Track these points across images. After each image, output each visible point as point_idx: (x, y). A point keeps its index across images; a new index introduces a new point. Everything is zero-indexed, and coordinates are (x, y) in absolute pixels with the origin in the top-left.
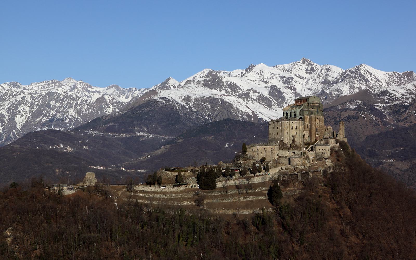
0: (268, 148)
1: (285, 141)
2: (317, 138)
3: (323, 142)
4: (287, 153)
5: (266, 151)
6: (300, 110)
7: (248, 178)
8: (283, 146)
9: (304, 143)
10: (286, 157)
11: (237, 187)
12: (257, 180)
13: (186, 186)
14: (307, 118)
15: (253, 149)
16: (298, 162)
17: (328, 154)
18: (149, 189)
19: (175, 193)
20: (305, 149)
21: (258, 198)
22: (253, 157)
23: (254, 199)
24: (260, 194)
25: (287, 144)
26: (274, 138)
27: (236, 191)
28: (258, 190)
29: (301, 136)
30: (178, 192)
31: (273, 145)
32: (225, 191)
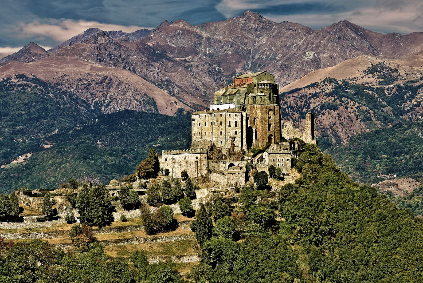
0: (191, 157)
1: (218, 145)
5: (187, 162)
15: (166, 160)
20: (250, 158)
25: (220, 151)
26: (200, 141)
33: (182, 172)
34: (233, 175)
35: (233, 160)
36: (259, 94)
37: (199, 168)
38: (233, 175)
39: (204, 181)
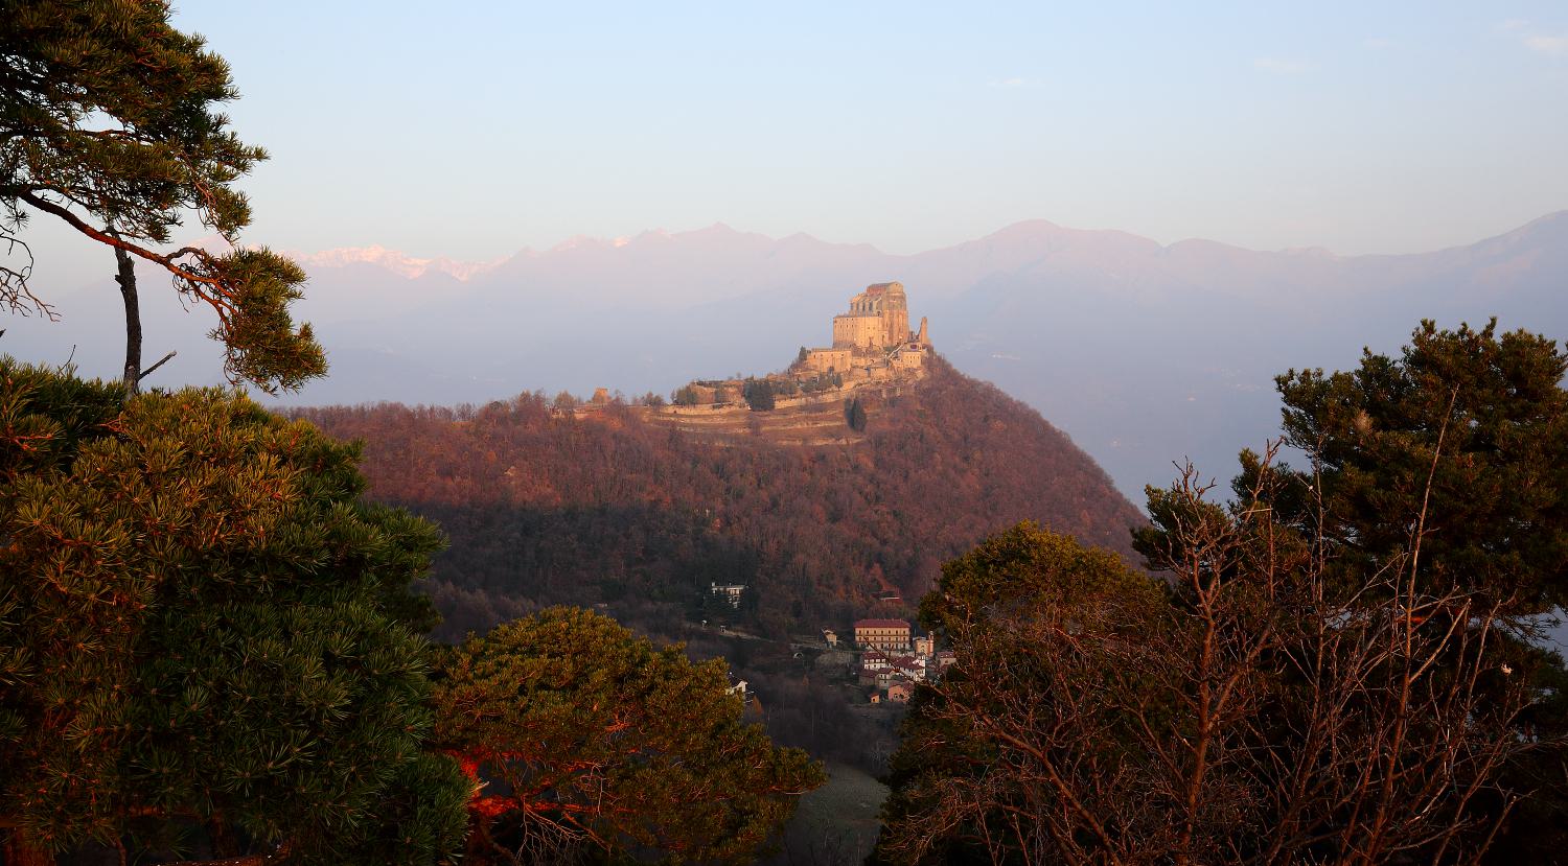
0: (838, 354)
3: (908, 346)
4: (862, 362)
7: (815, 396)
8: (857, 352)
10: (862, 367)
11: (802, 408)
12: (829, 398)
18: (681, 411)
22: (816, 366)
24: (833, 418)
27: (804, 414)
28: (829, 413)
30: (722, 416)
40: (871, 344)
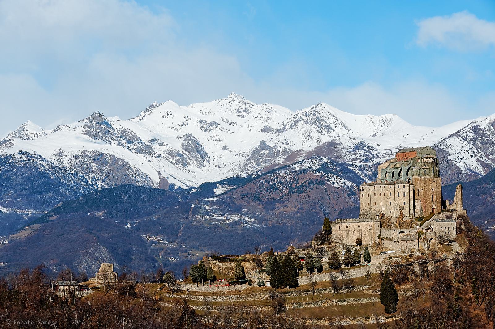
0: (365, 226)
2: (433, 211)
5: (361, 230)
6: (408, 168)
7: (342, 273)
9: (415, 217)
13: (250, 284)
14: (418, 180)
16: (413, 246)
17: (454, 234)
18: (194, 288)
19: (235, 292)
20: (418, 227)
21: (359, 302)
23: (353, 302)
25: (390, 220)
26: (369, 211)
29: (412, 206)
30: (240, 293)
31: (372, 222)
32: (308, 291)
33: (357, 239)
34: (407, 242)
35: (403, 228)
36: (423, 167)
37: (371, 235)
38: (407, 242)
39: (377, 247)
40: (402, 213)
